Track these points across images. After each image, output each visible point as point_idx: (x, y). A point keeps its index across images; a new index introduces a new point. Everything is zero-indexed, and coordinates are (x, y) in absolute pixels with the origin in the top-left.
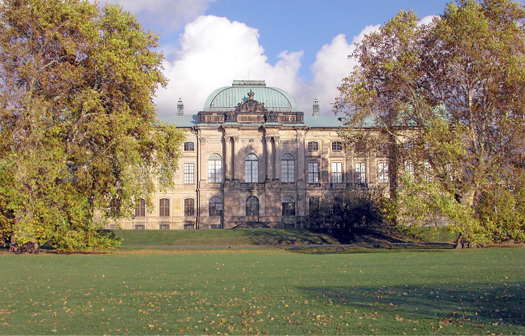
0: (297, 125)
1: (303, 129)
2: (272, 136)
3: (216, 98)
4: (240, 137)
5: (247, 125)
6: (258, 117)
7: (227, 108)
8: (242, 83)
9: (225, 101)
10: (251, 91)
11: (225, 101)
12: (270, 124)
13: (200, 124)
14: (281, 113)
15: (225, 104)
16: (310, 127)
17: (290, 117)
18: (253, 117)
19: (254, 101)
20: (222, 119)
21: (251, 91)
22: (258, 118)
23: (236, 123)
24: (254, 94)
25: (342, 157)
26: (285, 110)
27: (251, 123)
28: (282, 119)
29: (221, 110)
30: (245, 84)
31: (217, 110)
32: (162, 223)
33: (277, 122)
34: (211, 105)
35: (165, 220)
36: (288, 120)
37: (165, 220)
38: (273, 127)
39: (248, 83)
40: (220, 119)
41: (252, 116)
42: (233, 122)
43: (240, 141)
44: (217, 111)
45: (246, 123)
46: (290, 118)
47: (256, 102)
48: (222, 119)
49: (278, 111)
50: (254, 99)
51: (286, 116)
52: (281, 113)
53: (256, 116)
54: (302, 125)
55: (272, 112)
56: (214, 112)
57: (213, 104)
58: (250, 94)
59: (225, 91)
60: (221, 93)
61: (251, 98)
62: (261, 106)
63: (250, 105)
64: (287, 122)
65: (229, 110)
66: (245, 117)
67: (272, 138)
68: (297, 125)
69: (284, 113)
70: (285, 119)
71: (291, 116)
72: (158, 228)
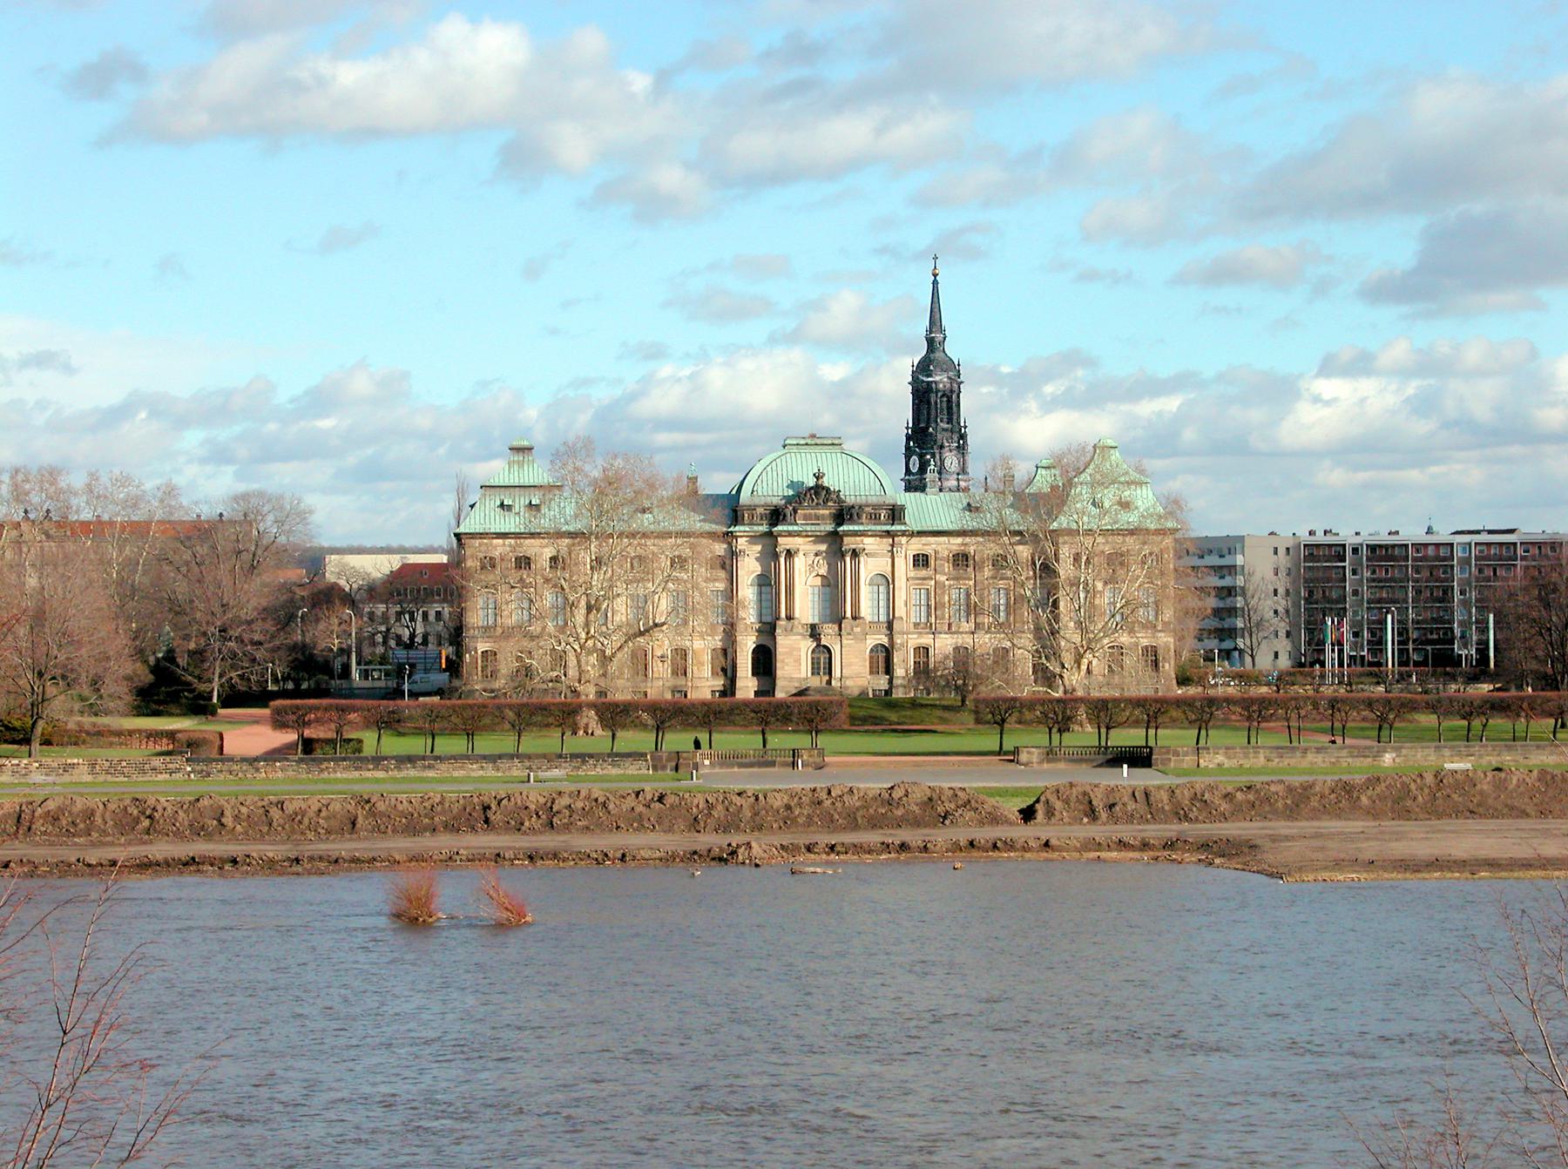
0: (893, 528)
1: (903, 535)
2: (854, 547)
4: (801, 548)
5: (813, 528)
8: (803, 442)
9: (775, 484)
11: (775, 484)
12: (851, 528)
13: (737, 528)
16: (916, 529)
19: (823, 488)
23: (796, 528)
24: (824, 474)
26: (874, 500)
30: (807, 444)
32: (675, 687)
33: (862, 524)
35: (681, 681)
37: (681, 681)
38: (855, 534)
41: (821, 512)
42: (792, 524)
43: (801, 554)
45: (812, 524)
47: (828, 489)
49: (864, 502)
50: (826, 484)
52: (868, 506)
54: (903, 528)
56: (759, 506)
60: (769, 469)
64: (877, 521)
66: (810, 514)
67: (854, 550)
68: (893, 528)
69: (876, 507)
72: (668, 696)
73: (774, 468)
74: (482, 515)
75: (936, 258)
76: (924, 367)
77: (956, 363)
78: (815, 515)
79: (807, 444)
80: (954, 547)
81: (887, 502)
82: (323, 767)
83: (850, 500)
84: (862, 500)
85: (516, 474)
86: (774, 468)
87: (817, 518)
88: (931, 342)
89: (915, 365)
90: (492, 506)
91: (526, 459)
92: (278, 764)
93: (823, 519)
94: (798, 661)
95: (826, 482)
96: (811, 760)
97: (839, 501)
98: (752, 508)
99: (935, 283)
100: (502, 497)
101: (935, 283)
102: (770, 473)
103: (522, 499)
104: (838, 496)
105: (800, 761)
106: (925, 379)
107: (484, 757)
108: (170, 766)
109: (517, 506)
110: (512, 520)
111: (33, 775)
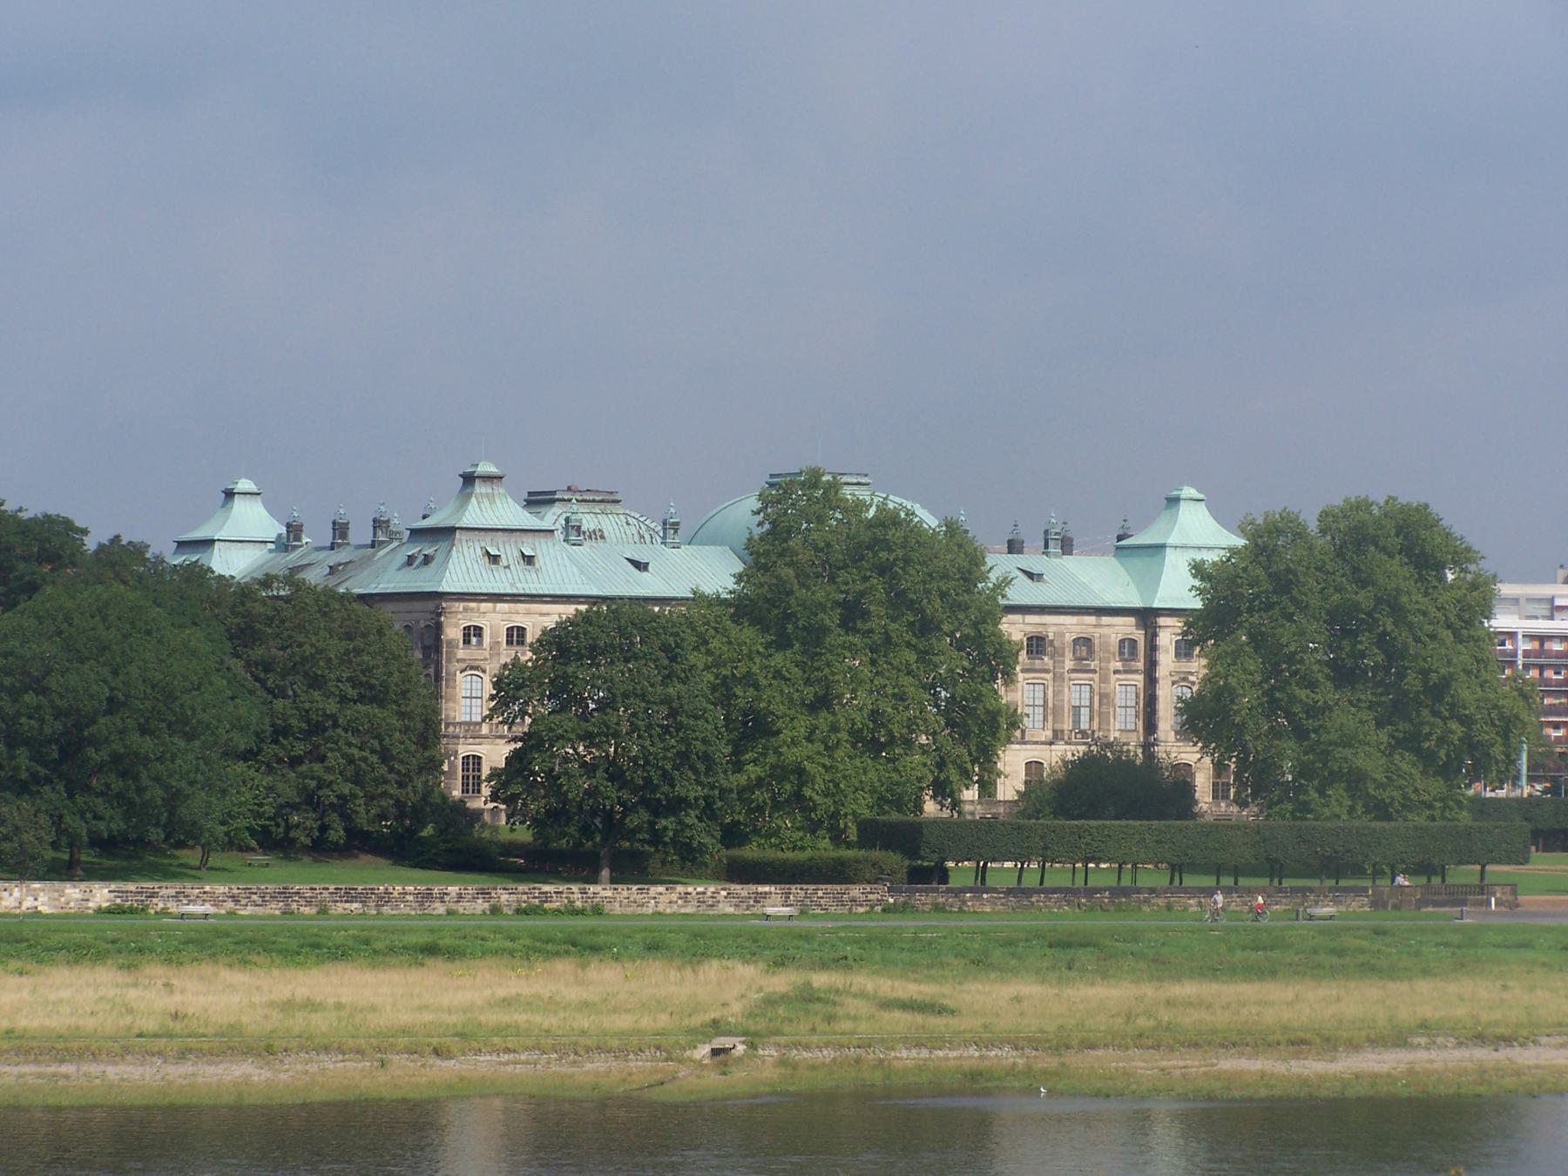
25: (1047, 671)
74: (464, 568)
80: (1029, 629)
82: (1034, 899)
85: (491, 513)
90: (473, 556)
91: (496, 492)
92: (985, 896)
96: (1504, 898)
100: (483, 544)
103: (508, 547)
105: (1493, 899)
107: (1055, 890)
108: (871, 897)
109: (503, 556)
110: (503, 576)
111: (721, 905)
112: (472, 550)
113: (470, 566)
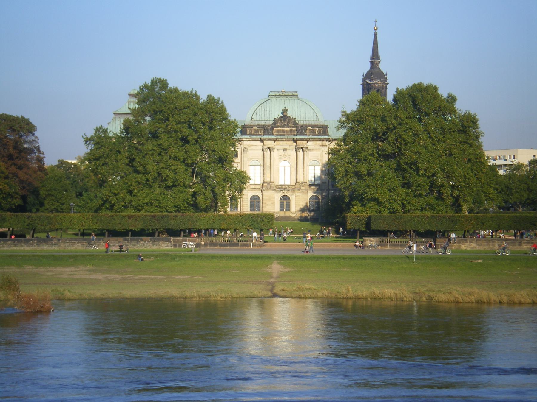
3: (256, 111)
6: (290, 129)
7: (265, 122)
8: (278, 94)
9: (263, 115)
10: (285, 108)
14: (309, 126)
15: (263, 118)
17: (317, 130)
18: (287, 130)
20: (261, 131)
21: (285, 108)
22: (291, 131)
23: (272, 137)
24: (287, 110)
26: (313, 123)
27: (284, 135)
28: (310, 132)
29: (260, 123)
30: (280, 95)
31: (257, 123)
33: (306, 135)
34: (252, 118)
36: (315, 132)
39: (283, 94)
40: (259, 132)
41: (286, 129)
42: (270, 135)
43: (276, 150)
44: (257, 124)
46: (317, 130)
47: (289, 117)
48: (261, 131)
49: (308, 124)
51: (314, 129)
53: (289, 129)
54: (326, 137)
55: (302, 126)
56: (254, 126)
57: (253, 117)
58: (284, 111)
59: (263, 104)
60: (260, 107)
61: (285, 114)
62: (294, 120)
63: (285, 120)
65: (267, 123)
66: (280, 130)
69: (314, 126)
70: (313, 131)
71: (318, 129)
73: (263, 107)
75: (376, 21)
76: (368, 76)
77: (385, 74)
78: (283, 130)
79: (280, 95)
81: (319, 124)
83: (301, 123)
84: (307, 123)
86: (263, 107)
87: (284, 132)
88: (372, 63)
89: (364, 75)
93: (286, 133)
94: (273, 203)
95: (289, 114)
97: (295, 123)
98: (251, 127)
99: (375, 35)
101: (375, 35)
102: (260, 109)
104: (295, 121)
106: (369, 82)
112: (119, 121)
113: (116, 127)
